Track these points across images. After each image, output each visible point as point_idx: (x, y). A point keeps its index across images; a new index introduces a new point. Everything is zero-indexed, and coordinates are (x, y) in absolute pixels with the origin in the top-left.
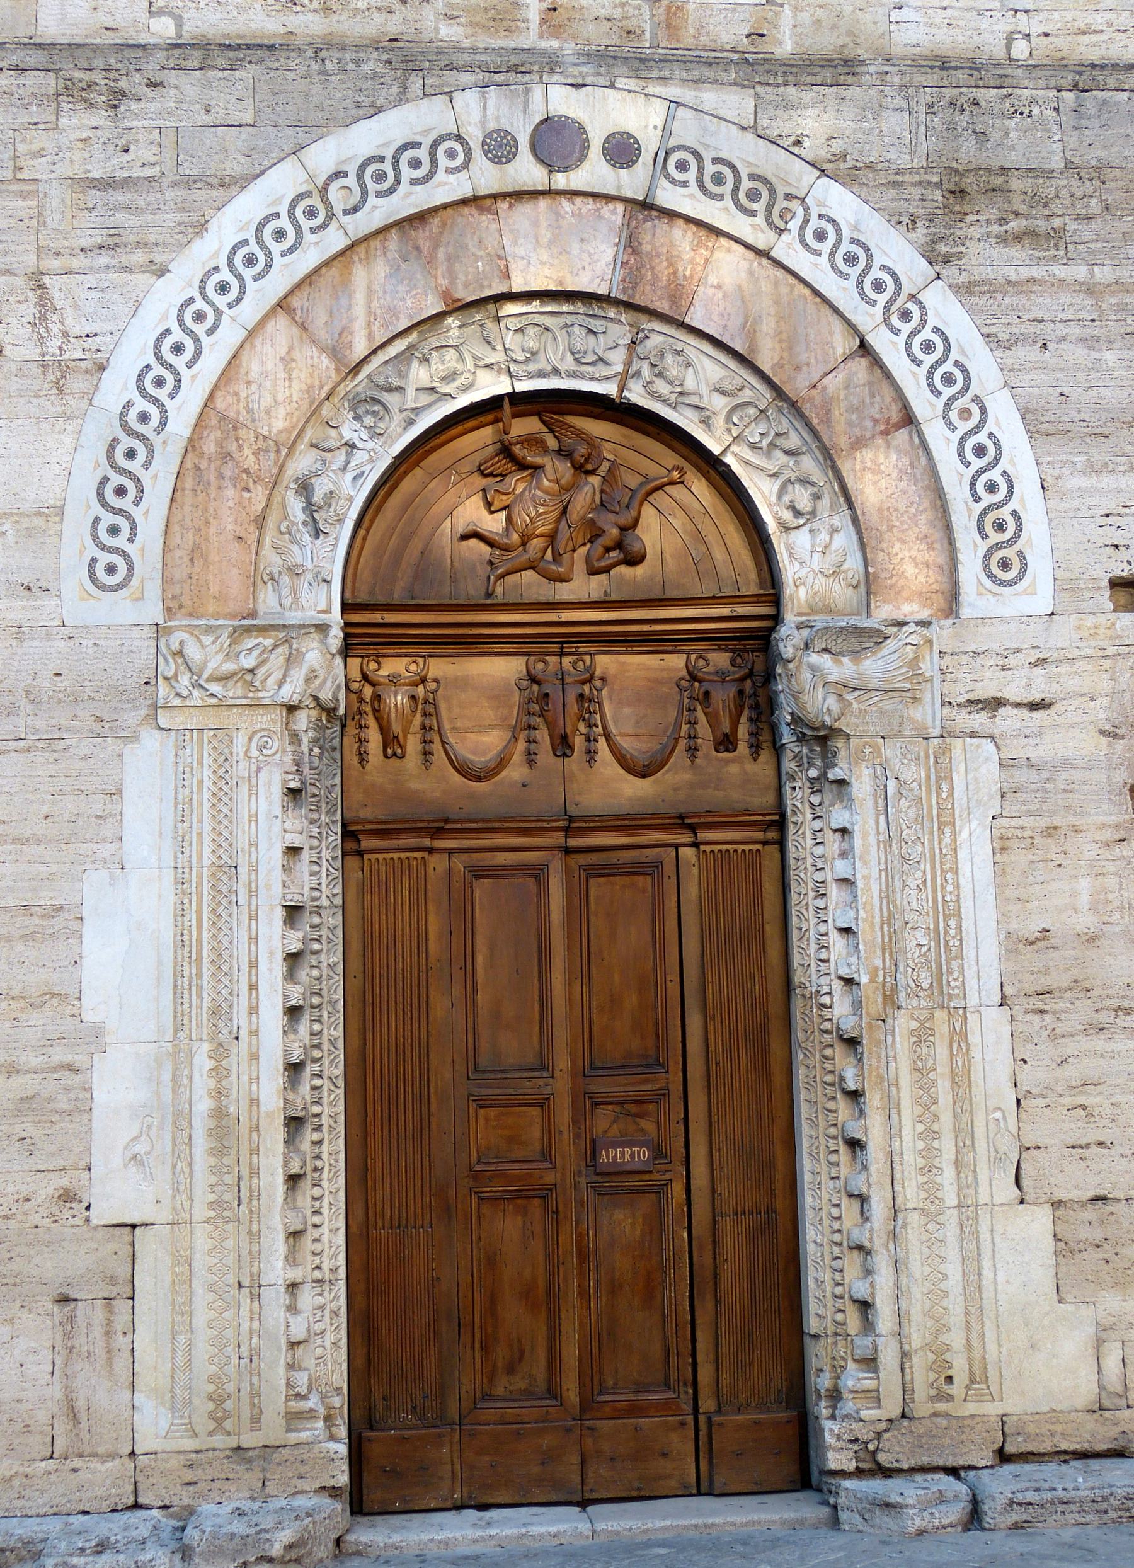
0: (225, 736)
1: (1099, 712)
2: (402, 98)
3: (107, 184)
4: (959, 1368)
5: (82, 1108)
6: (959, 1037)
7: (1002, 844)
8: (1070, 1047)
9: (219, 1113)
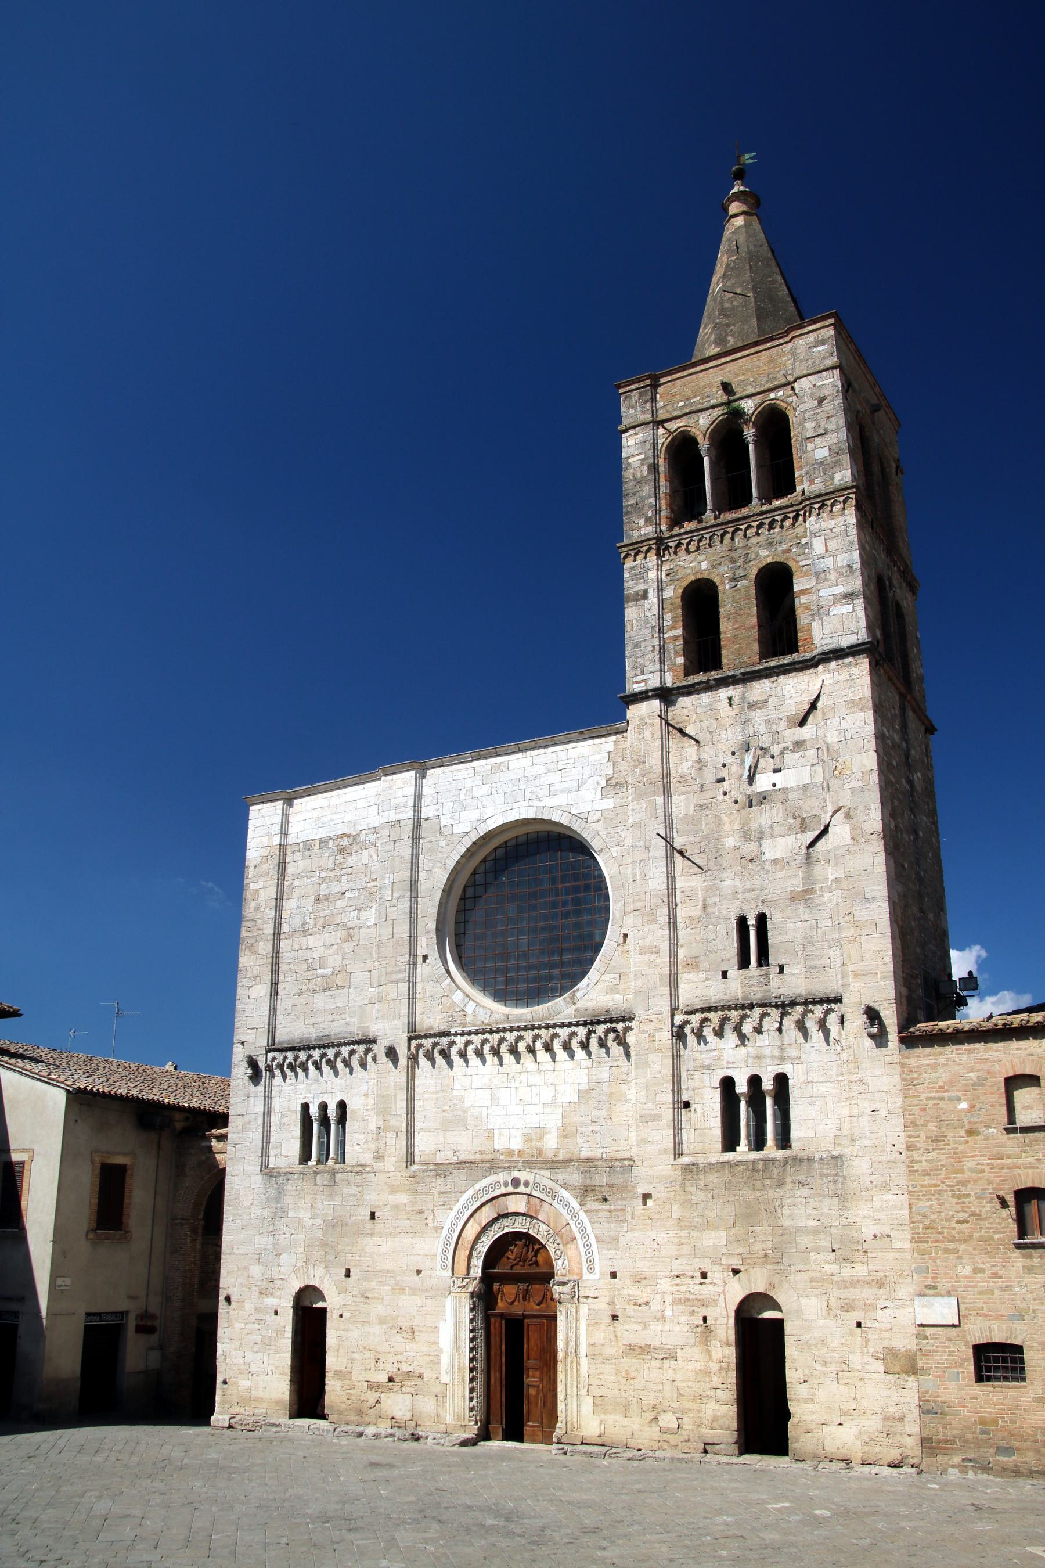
0: (460, 1298)
1: (607, 1300)
2: (490, 1175)
3: (444, 1193)
4: (576, 1426)
5: (439, 1363)
6: (578, 1363)
7: (588, 1325)
8: (598, 1366)
9: (459, 1366)
